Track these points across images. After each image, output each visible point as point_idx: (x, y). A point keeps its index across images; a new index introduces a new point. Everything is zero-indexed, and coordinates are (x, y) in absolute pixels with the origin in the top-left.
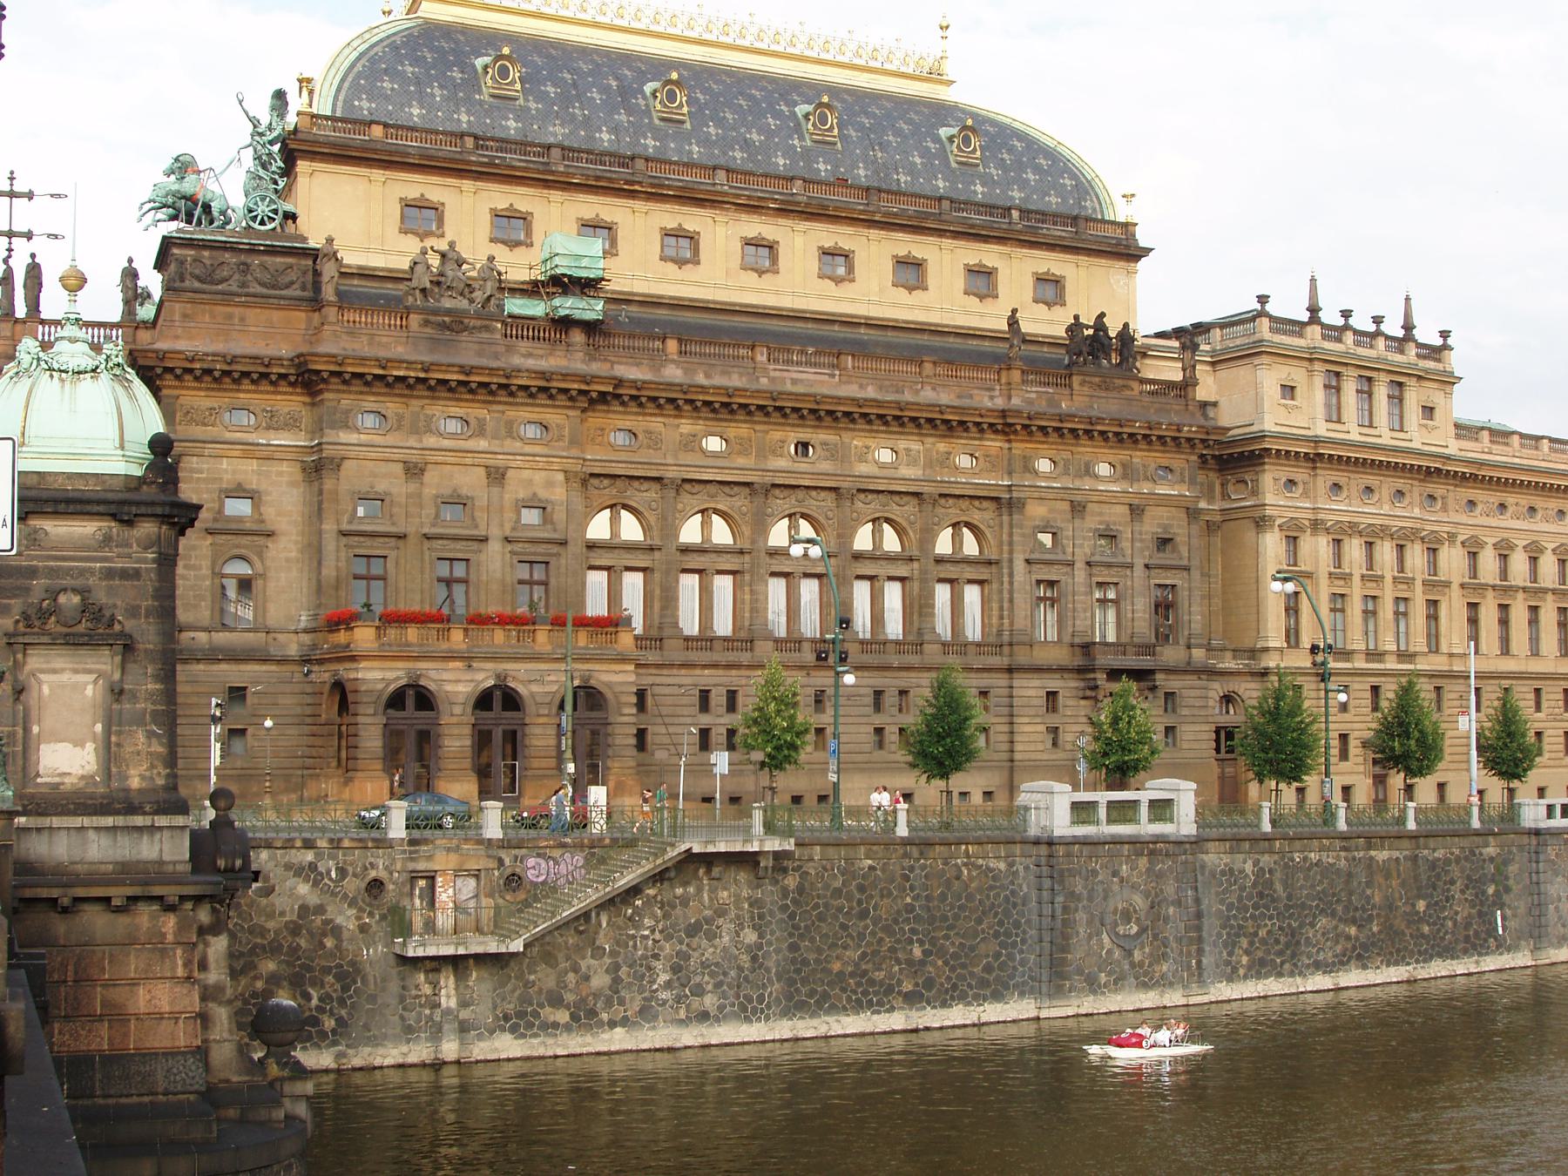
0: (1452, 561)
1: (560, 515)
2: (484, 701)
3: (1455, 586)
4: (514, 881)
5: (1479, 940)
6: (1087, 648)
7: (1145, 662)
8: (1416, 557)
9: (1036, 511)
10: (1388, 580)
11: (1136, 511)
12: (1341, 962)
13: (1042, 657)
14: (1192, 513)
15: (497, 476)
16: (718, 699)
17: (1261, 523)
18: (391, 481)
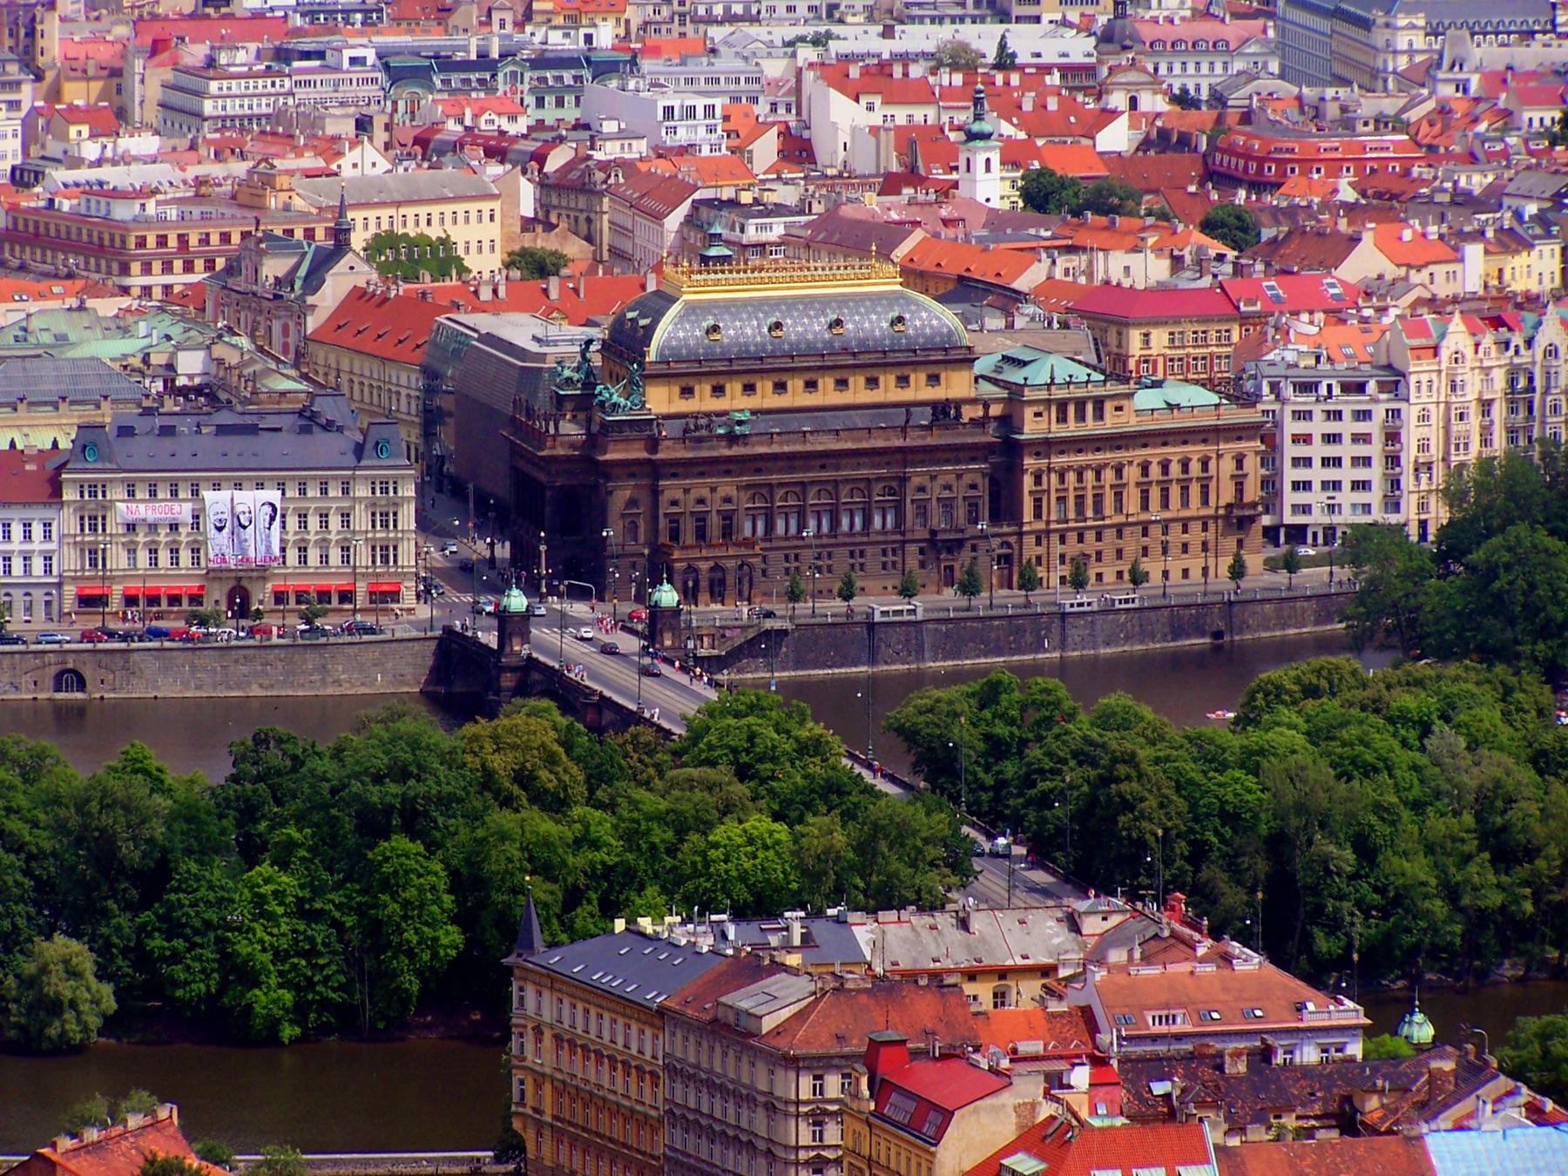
0: (1132, 474)
1: (735, 500)
2: (712, 569)
3: (1132, 484)
4: (723, 636)
5: (1040, 648)
6: (933, 533)
7: (959, 536)
8: (1109, 476)
9: (916, 481)
10: (1089, 487)
11: (959, 477)
12: (978, 656)
13: (917, 536)
14: (984, 475)
15: (713, 490)
16: (792, 557)
17: (1023, 472)
18: (679, 495)
